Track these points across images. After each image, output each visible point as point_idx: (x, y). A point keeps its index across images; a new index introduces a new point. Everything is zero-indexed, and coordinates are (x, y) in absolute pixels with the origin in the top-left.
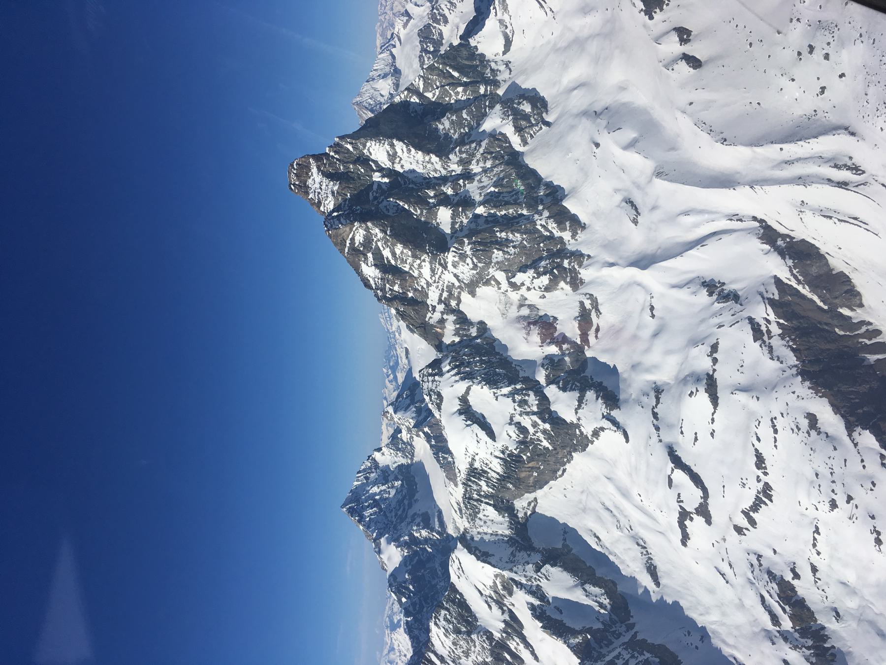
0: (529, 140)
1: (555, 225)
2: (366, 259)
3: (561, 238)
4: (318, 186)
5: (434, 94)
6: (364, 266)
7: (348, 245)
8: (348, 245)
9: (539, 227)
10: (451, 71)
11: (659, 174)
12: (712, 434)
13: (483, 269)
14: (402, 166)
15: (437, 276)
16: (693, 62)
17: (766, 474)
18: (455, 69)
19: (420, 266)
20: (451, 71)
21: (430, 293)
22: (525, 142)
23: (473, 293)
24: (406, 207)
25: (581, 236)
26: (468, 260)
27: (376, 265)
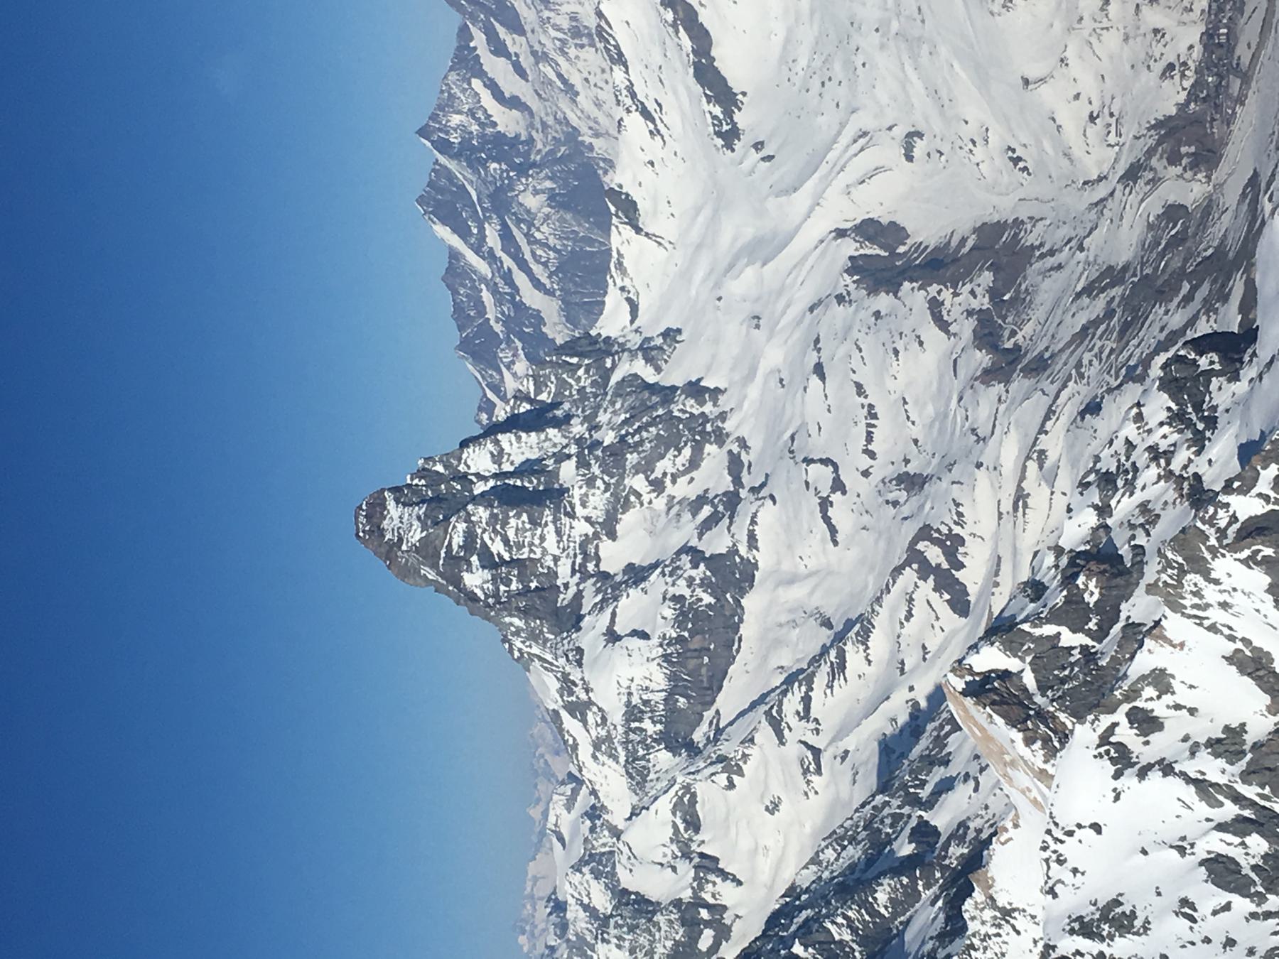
0: (664, 366)
1: (692, 401)
2: (469, 564)
3: (703, 413)
4: (397, 521)
5: (549, 393)
6: (466, 576)
7: (443, 555)
8: (443, 555)
9: (676, 413)
10: (567, 359)
11: (764, 264)
12: (829, 411)
13: (618, 484)
14: (512, 463)
15: (565, 538)
16: (769, 158)
17: (866, 397)
18: (572, 356)
19: (542, 538)
20: (567, 359)
21: (560, 570)
22: (658, 370)
23: (612, 535)
24: (519, 483)
25: (722, 399)
26: (599, 483)
27: (483, 567)
